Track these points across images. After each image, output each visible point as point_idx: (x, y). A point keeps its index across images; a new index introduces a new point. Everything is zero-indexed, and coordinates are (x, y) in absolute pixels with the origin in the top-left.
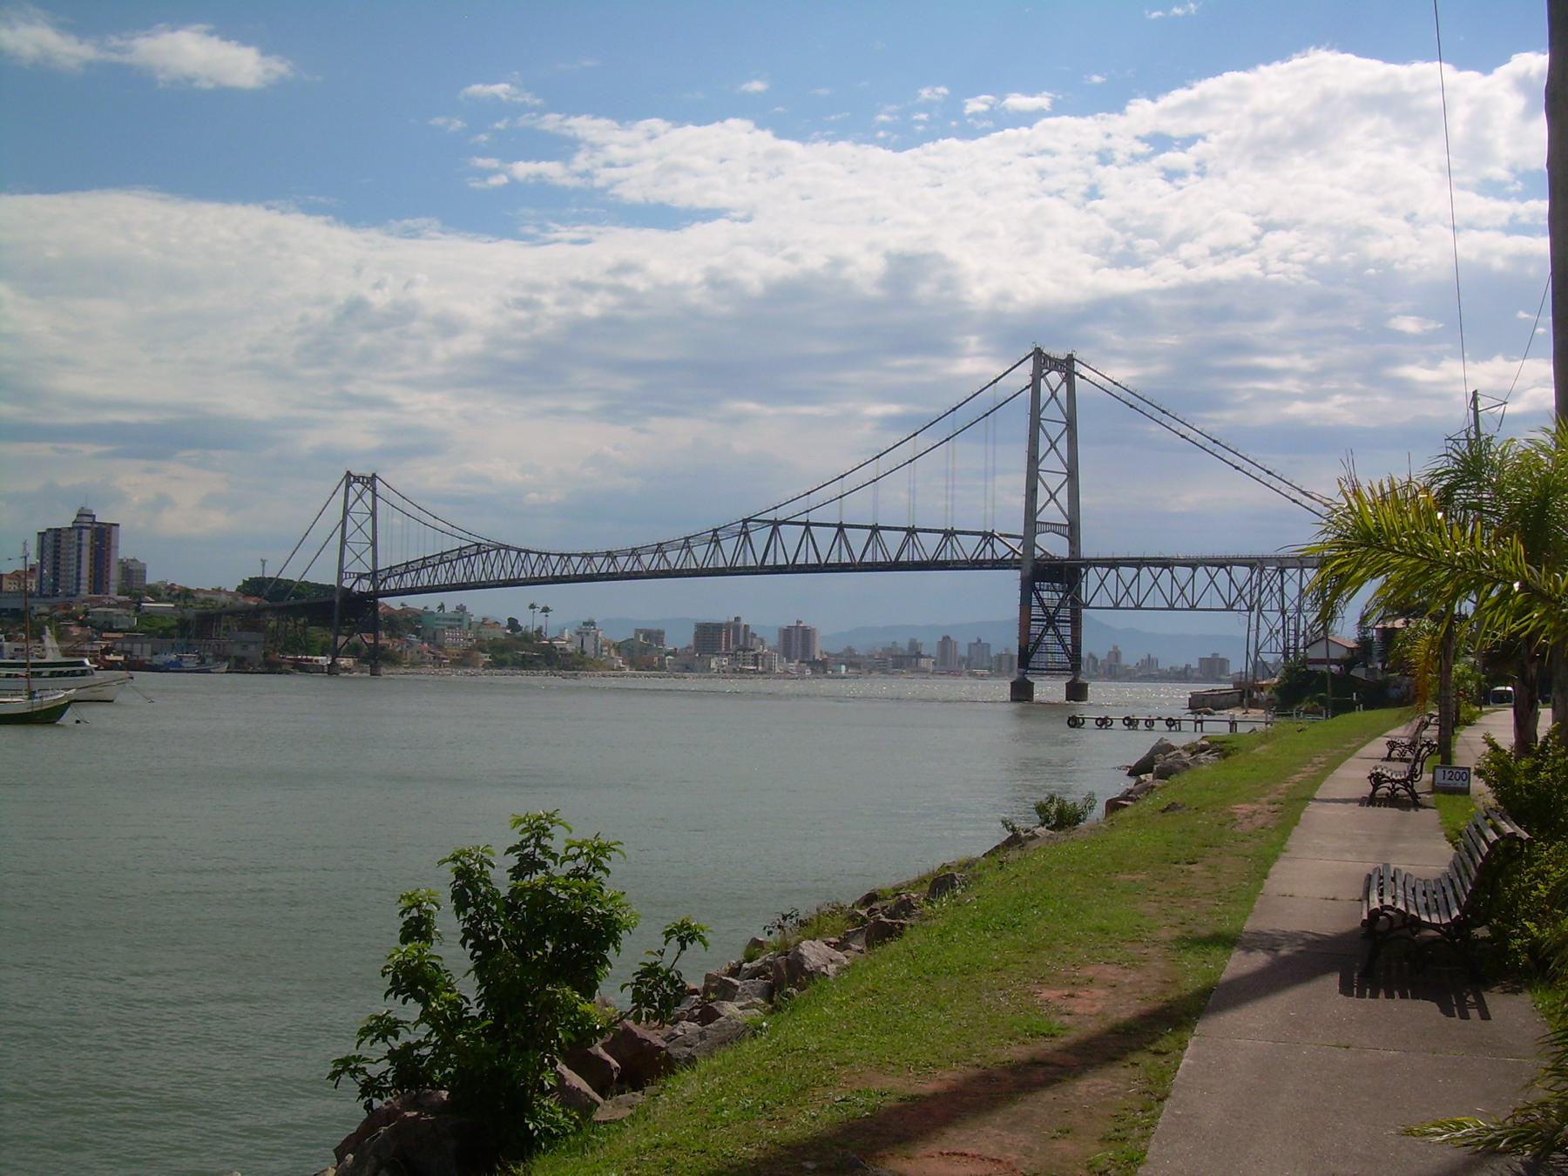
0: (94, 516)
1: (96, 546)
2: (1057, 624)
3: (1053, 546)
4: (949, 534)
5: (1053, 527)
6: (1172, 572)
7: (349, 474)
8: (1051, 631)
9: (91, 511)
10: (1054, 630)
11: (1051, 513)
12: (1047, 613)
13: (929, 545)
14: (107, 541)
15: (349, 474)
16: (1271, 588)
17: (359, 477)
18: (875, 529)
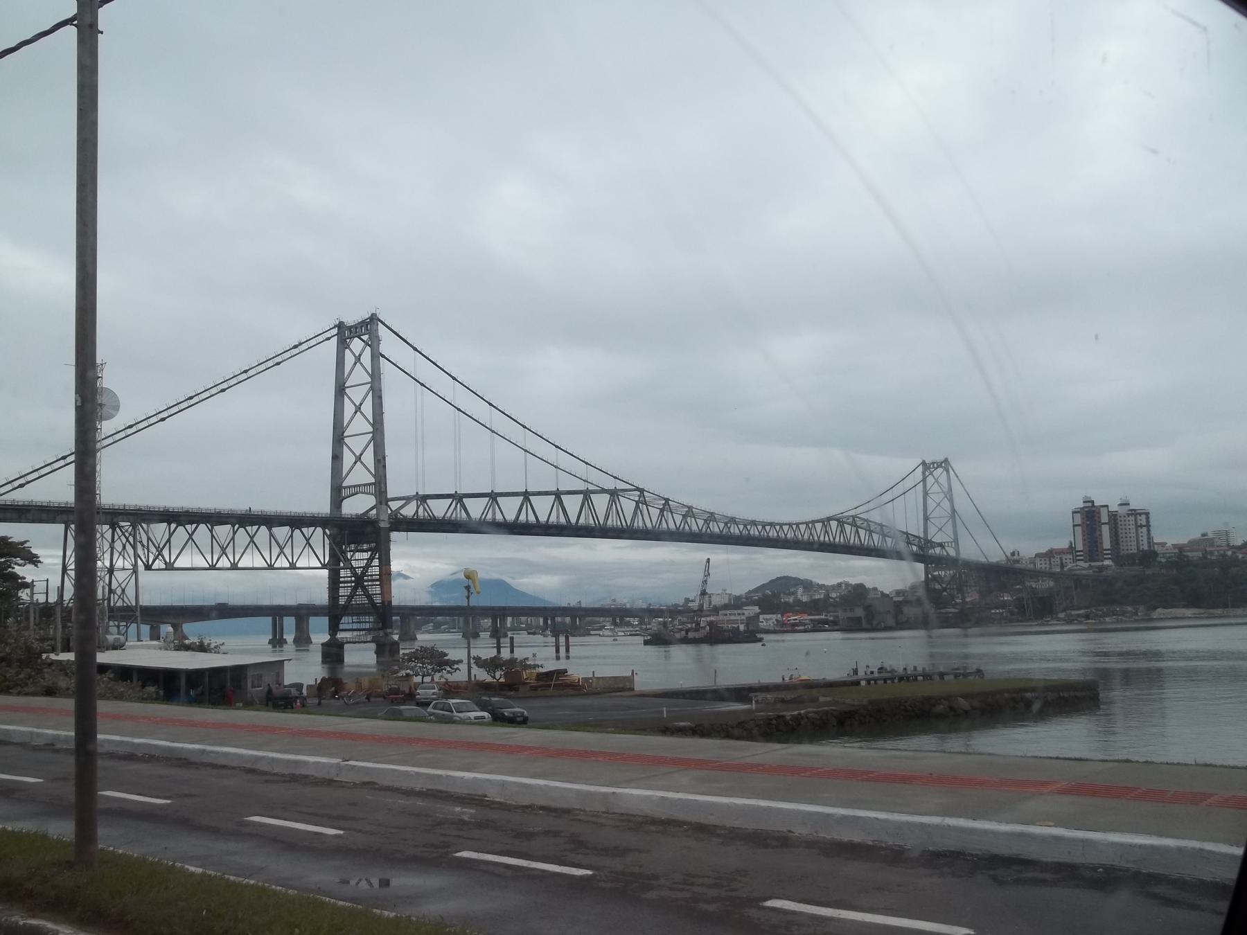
0: (1093, 502)
1: (1087, 525)
2: (366, 584)
3: (356, 506)
4: (493, 497)
5: (357, 489)
6: (235, 533)
7: (924, 463)
8: (360, 591)
9: (1090, 498)
10: (363, 591)
11: (360, 476)
12: (355, 574)
13: (509, 509)
14: (1097, 520)
15: (924, 463)
16: (143, 545)
17: (933, 463)
18: (526, 495)
